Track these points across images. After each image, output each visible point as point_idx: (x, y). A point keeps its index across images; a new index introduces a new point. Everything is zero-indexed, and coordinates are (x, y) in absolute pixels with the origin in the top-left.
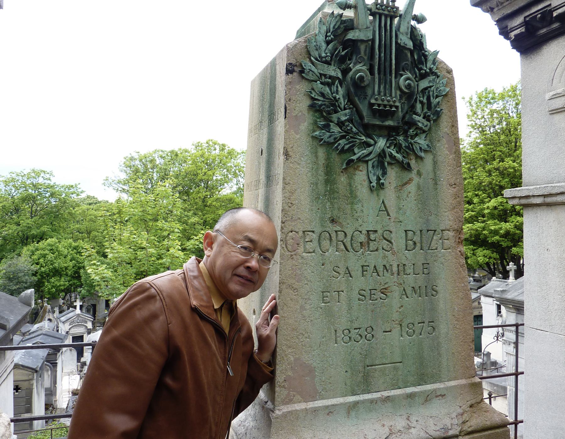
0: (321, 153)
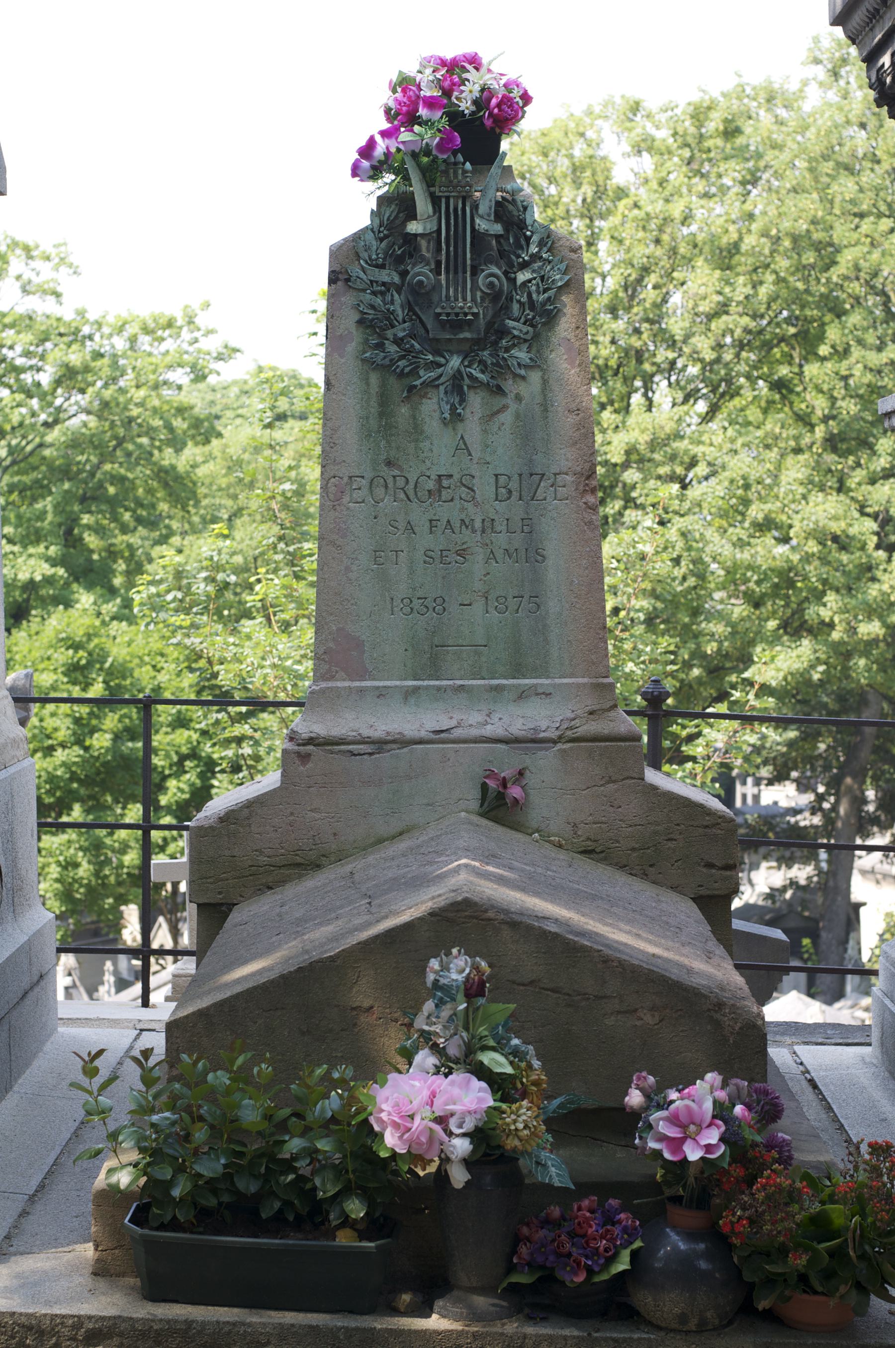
0: (374, 379)
